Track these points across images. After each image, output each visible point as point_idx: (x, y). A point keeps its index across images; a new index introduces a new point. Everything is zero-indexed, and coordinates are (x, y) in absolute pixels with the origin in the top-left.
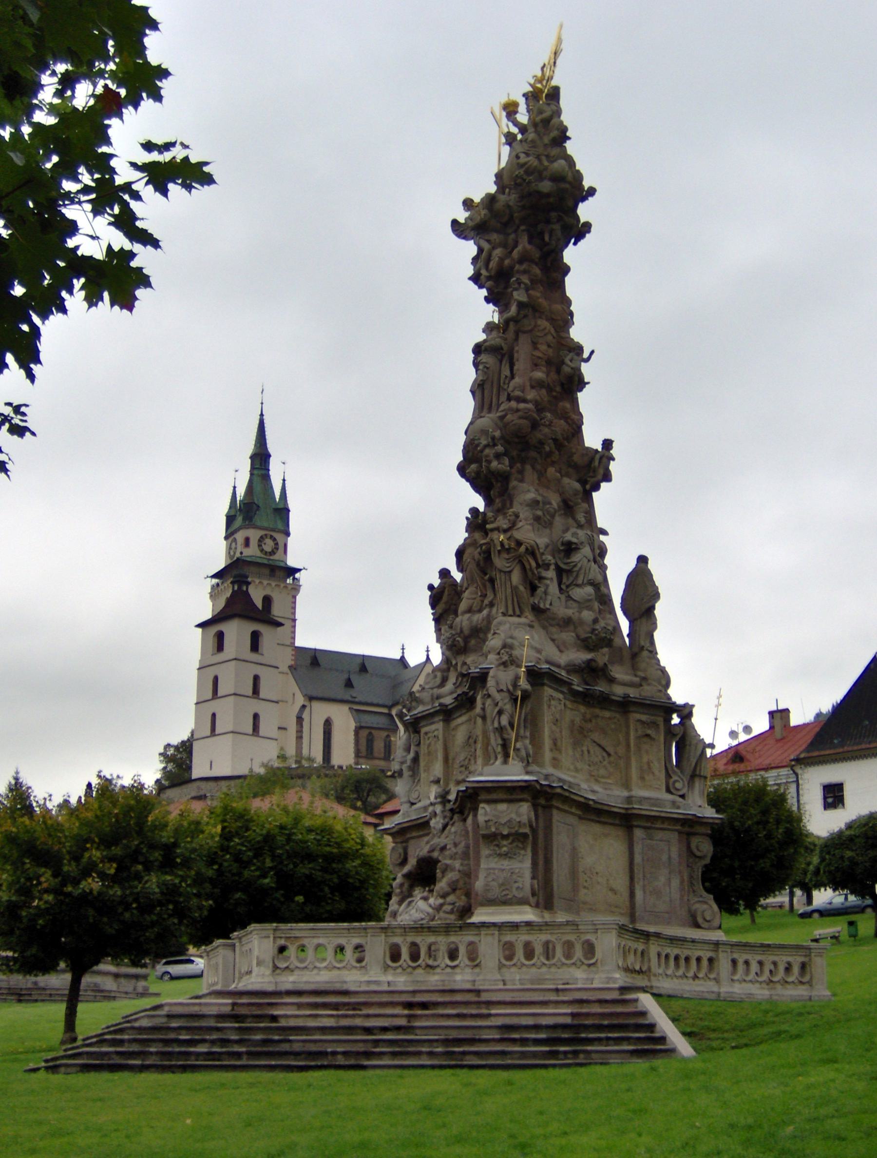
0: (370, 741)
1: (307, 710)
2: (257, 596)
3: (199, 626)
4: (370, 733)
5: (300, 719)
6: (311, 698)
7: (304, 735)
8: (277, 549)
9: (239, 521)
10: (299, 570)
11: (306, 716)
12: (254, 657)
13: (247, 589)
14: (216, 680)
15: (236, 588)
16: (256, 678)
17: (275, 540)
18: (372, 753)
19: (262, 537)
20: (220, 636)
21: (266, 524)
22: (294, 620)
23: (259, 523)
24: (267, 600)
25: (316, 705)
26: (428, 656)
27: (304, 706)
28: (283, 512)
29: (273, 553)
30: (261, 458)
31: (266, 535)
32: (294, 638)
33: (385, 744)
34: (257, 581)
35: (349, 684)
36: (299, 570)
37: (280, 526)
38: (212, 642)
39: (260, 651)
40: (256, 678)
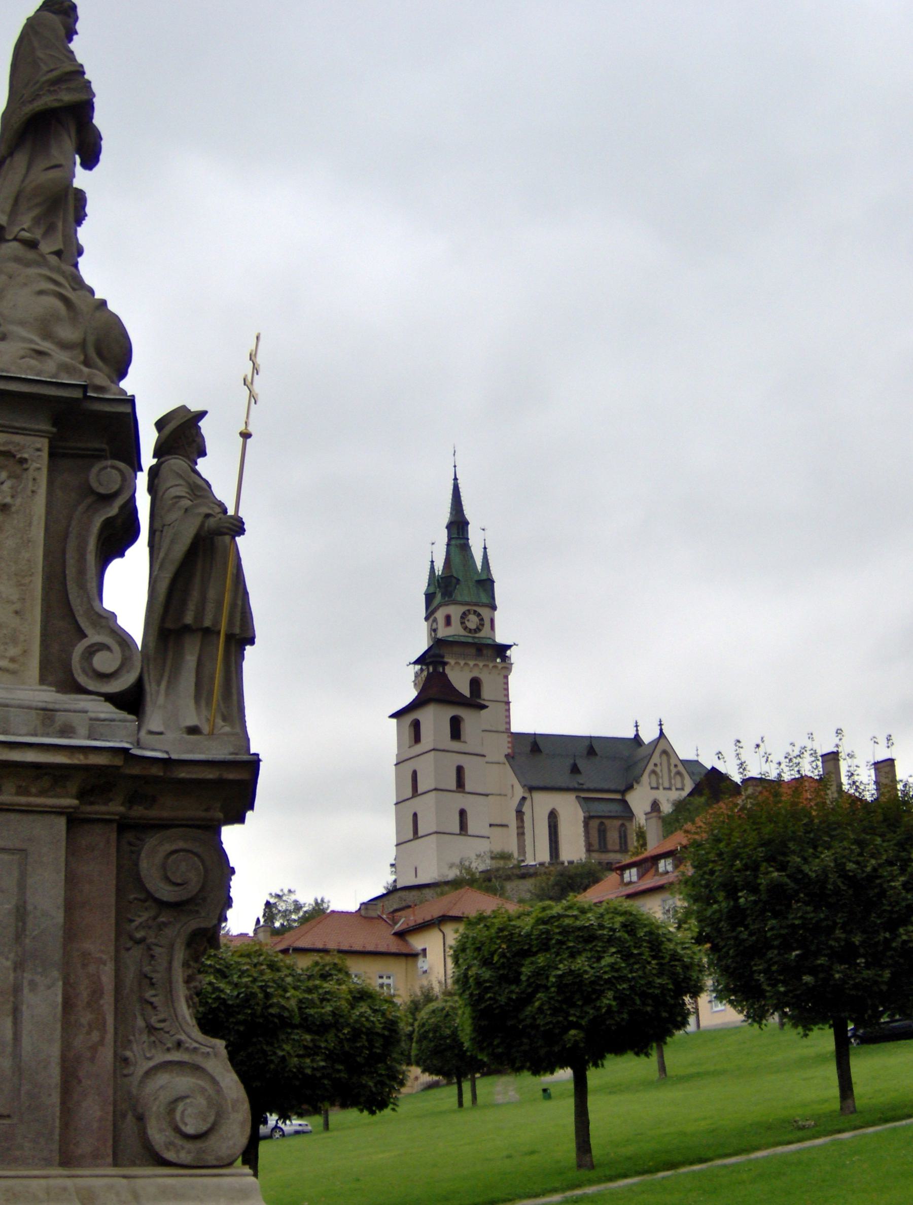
0: (602, 832)
1: (528, 803)
2: (459, 678)
3: (393, 716)
4: (602, 824)
5: (520, 813)
6: (531, 789)
7: (526, 830)
8: (483, 625)
9: (438, 598)
10: (509, 647)
11: (526, 809)
12: (456, 746)
13: (444, 669)
14: (415, 774)
15: (431, 669)
16: (460, 770)
17: (479, 615)
18: (605, 844)
19: (464, 613)
20: (416, 725)
21: (467, 599)
22: (508, 703)
23: (459, 599)
24: (475, 684)
25: (538, 796)
26: (661, 730)
27: (524, 799)
28: (486, 584)
29: (478, 630)
30: (458, 526)
31: (469, 611)
32: (509, 723)
33: (620, 832)
34: (452, 662)
35: (575, 770)
36: (509, 647)
37: (484, 599)
38: (408, 732)
39: (462, 739)
40: (460, 770)
